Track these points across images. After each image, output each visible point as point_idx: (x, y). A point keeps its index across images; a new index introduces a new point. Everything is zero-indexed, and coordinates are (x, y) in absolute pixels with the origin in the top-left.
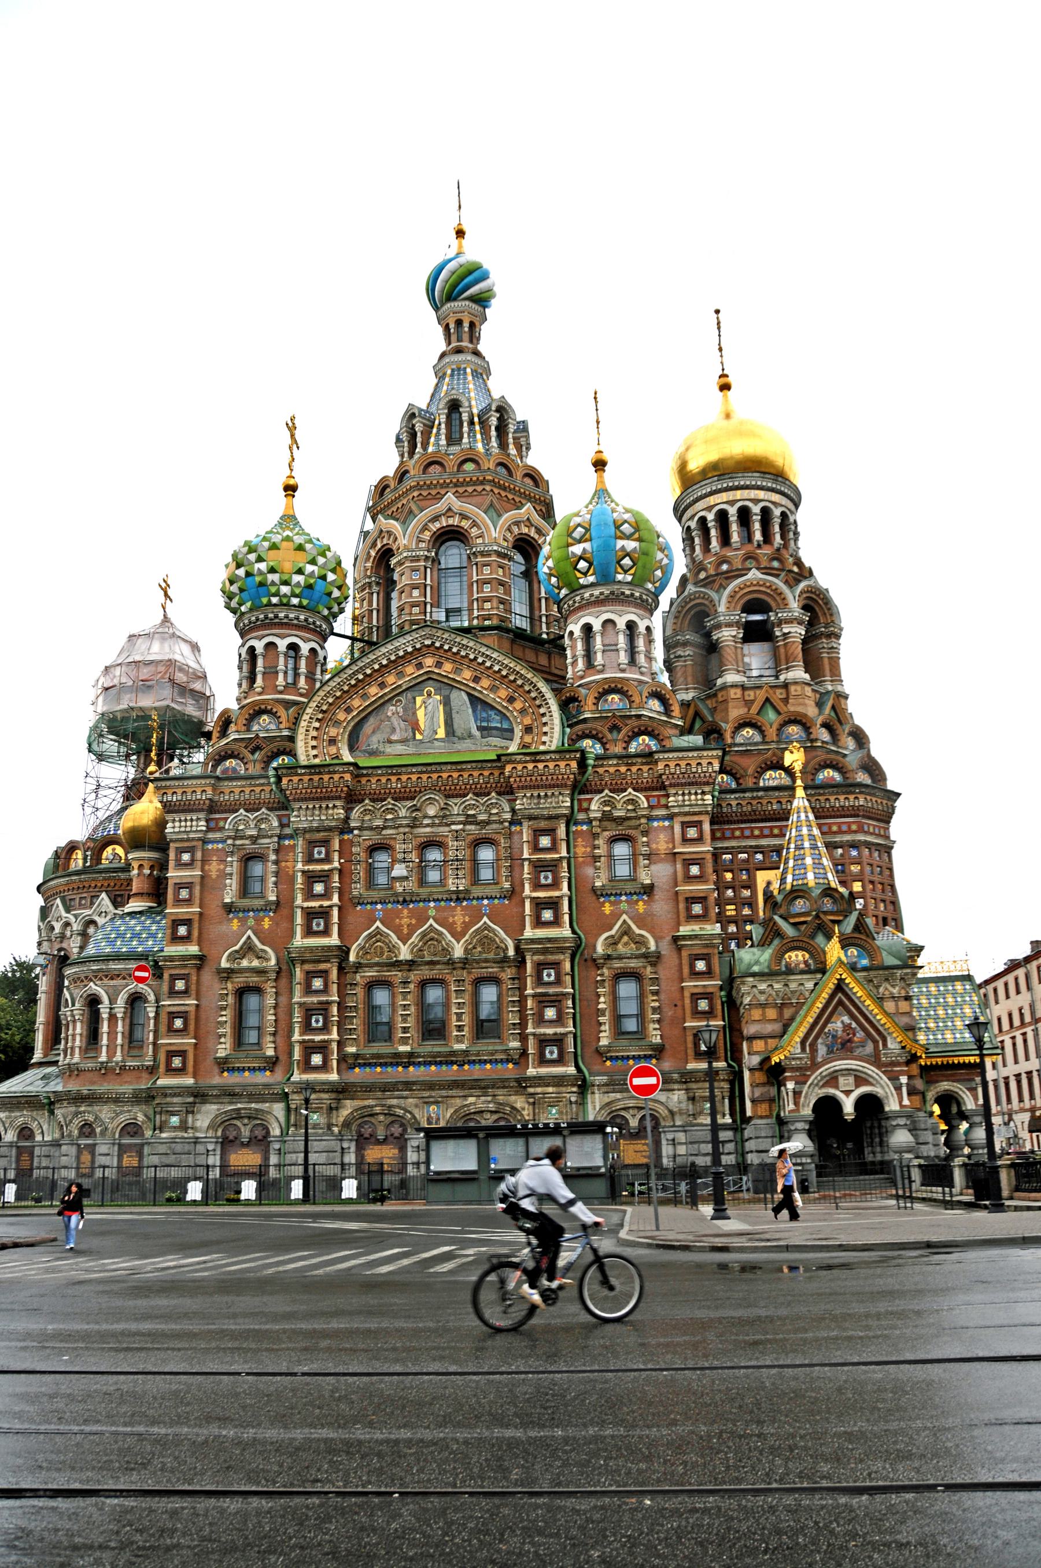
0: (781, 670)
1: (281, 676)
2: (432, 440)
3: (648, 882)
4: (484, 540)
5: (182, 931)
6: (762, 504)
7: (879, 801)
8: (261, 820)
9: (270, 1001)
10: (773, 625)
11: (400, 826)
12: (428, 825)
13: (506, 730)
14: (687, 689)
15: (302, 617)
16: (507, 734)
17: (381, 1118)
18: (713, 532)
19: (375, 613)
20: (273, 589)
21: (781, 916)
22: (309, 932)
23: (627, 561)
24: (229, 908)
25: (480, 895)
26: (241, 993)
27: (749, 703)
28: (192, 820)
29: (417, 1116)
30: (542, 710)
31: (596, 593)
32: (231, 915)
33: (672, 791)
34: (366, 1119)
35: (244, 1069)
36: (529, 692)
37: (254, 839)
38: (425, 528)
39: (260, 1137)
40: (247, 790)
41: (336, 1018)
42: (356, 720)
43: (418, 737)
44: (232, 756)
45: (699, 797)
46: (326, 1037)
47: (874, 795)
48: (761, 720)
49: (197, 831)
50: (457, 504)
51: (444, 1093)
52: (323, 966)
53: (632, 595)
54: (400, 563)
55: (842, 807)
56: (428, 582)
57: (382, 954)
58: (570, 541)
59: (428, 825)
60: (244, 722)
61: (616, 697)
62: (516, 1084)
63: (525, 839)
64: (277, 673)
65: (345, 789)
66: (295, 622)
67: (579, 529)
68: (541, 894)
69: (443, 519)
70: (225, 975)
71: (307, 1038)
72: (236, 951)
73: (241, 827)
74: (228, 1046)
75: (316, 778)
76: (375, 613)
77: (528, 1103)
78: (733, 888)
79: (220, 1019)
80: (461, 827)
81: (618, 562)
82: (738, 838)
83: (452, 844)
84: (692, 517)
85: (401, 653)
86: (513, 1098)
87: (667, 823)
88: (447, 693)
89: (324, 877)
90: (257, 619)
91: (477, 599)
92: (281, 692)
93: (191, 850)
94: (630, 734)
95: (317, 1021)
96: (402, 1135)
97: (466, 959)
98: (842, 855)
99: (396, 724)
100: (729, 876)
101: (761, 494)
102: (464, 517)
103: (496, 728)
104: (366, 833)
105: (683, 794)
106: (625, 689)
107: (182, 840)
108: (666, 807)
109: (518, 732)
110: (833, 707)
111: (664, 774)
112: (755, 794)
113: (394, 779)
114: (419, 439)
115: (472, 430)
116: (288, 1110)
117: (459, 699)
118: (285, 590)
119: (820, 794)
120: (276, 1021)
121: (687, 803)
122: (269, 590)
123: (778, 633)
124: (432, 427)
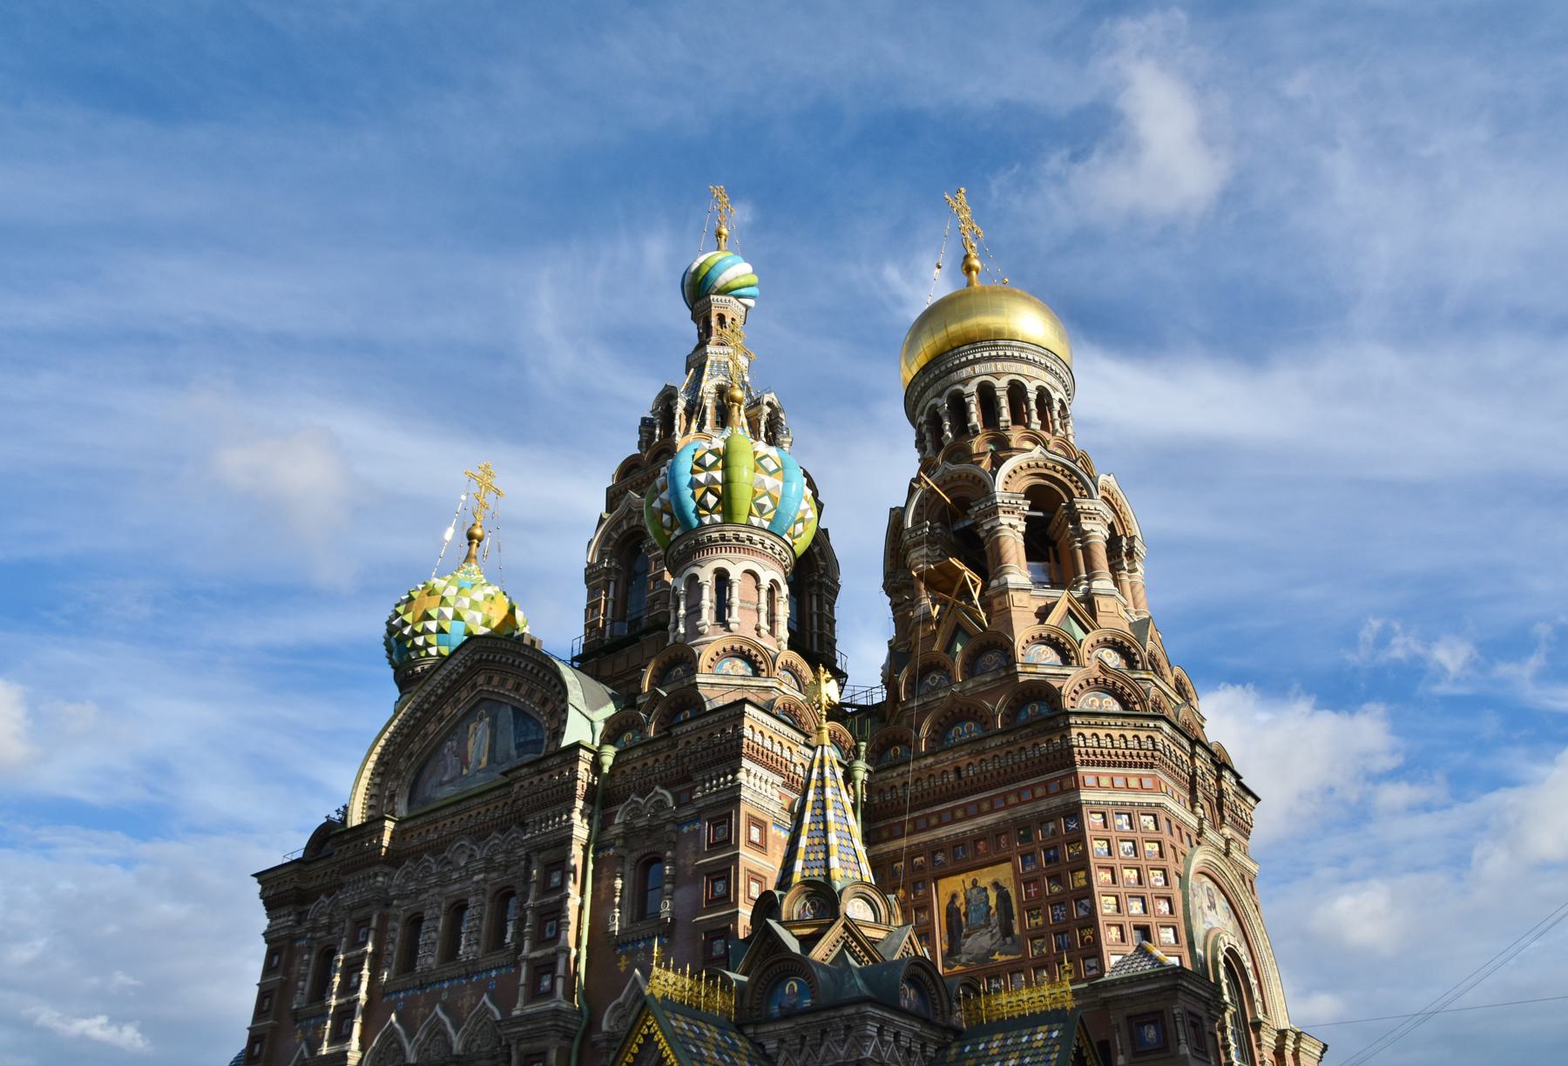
12: (456, 881)
31: (682, 547)
43: (465, 771)
53: (723, 538)
68: (538, 954)
69: (624, 522)
80: (482, 876)
83: (472, 900)
85: (454, 676)
101: (977, 367)
103: (533, 742)
104: (406, 902)
109: (546, 742)
110: (1070, 612)
113: (432, 828)
117: (506, 714)
123: (982, 535)
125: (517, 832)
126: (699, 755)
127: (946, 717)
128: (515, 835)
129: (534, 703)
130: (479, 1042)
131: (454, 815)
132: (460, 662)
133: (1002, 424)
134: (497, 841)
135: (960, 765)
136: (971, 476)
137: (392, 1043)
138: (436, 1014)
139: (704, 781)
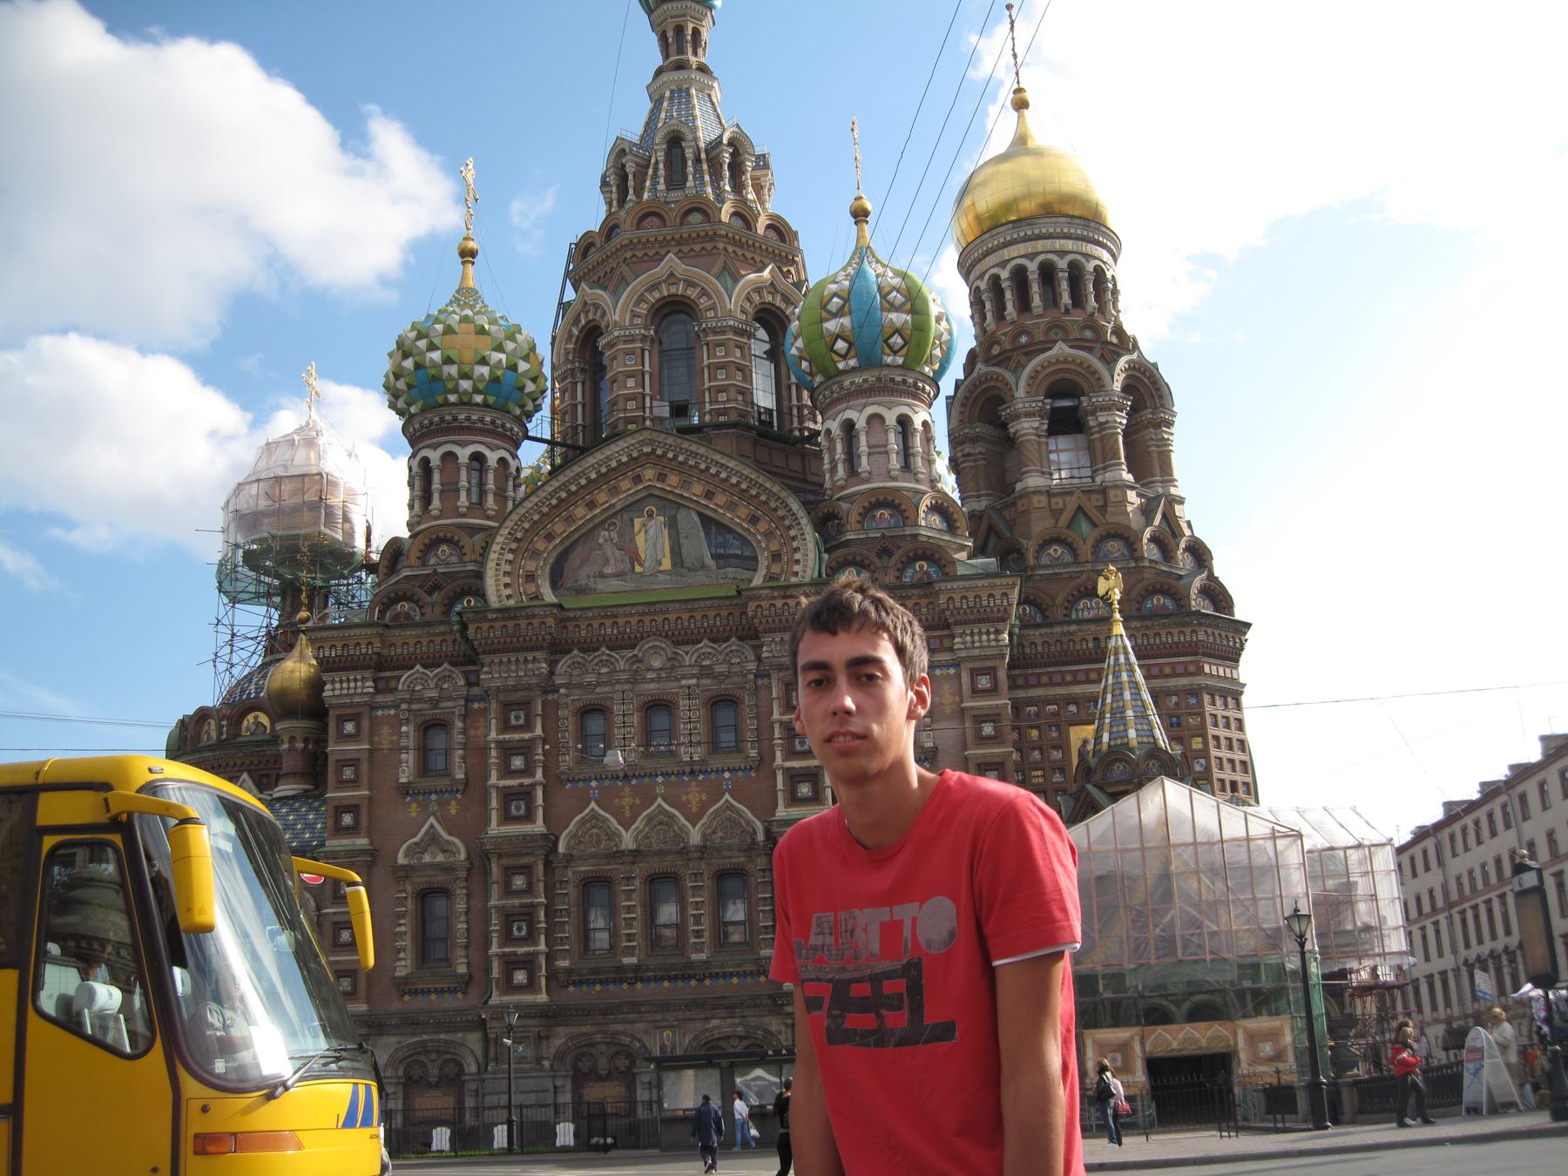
0: (1097, 470)
1: (463, 495)
2: (648, 183)
3: (930, 745)
4: (716, 313)
5: (347, 819)
6: (1070, 257)
7: (1223, 634)
8: (444, 678)
9: (461, 906)
10: (1087, 413)
11: (618, 682)
12: (652, 680)
13: (747, 558)
14: (979, 496)
15: (488, 419)
16: (751, 562)
17: (603, 1048)
18: (1008, 295)
19: (580, 408)
20: (450, 385)
21: (1095, 785)
22: (506, 818)
23: (897, 340)
24: (405, 790)
25: (720, 766)
26: (425, 896)
27: (1056, 514)
28: (356, 680)
29: (648, 1045)
30: (793, 533)
31: (858, 380)
32: (409, 799)
33: (958, 630)
34: (584, 1050)
35: (429, 991)
36: (775, 510)
37: (435, 703)
38: (641, 299)
39: (451, 1076)
40: (424, 641)
41: (543, 925)
42: (560, 549)
43: (638, 569)
44: (405, 598)
45: (992, 637)
46: (531, 949)
47: (1217, 626)
48: (1071, 535)
49: (362, 694)
50: (681, 268)
51: (680, 1015)
52: (525, 860)
53: (904, 382)
54: (611, 345)
55: (1177, 644)
56: (647, 368)
57: (599, 842)
58: (824, 314)
59: (652, 680)
60: (419, 554)
61: (886, 513)
62: (769, 1002)
63: (774, 695)
64: (458, 490)
65: (548, 637)
66: (479, 425)
67: (835, 300)
70: (403, 874)
71: (507, 950)
72: (415, 843)
73: (417, 688)
74: (409, 962)
75: (511, 624)
76: (580, 408)
77: (786, 1025)
78: (1040, 749)
79: (398, 929)
80: (694, 681)
81: (886, 341)
82: (1045, 685)
83: (683, 703)
84: (981, 277)
85: (614, 464)
86: (766, 1019)
87: (952, 671)
88: (673, 513)
89: (525, 749)
90: (431, 423)
91: (709, 389)
92: (463, 516)
93: (355, 718)
94: (904, 559)
95: (520, 929)
96: (629, 1069)
97: (704, 846)
98: (1177, 704)
99: (609, 553)
100: (1035, 733)
101: (1069, 245)
102: (690, 284)
103: (735, 556)
104: (575, 691)
105: (972, 634)
106: (897, 502)
107: (344, 706)
108: (951, 649)
109: (763, 562)
111: (948, 609)
112: (1066, 629)
113: (608, 622)
114: (631, 183)
115: (698, 172)
116: (486, 1040)
117: (689, 521)
118: (465, 385)
119: (1147, 627)
120: (468, 930)
121: (977, 644)
122: (445, 387)
123: (1092, 423)
124: (647, 167)
125: (739, 645)
126: (962, 612)
127: (1079, 590)
128: (734, 648)
129: (738, 517)
130: (720, 834)
131: (643, 614)
132: (623, 450)
133: (1090, 310)
134: (709, 650)
135: (1099, 636)
136: (1086, 365)
137: (593, 827)
138: (660, 805)
139: (963, 634)
